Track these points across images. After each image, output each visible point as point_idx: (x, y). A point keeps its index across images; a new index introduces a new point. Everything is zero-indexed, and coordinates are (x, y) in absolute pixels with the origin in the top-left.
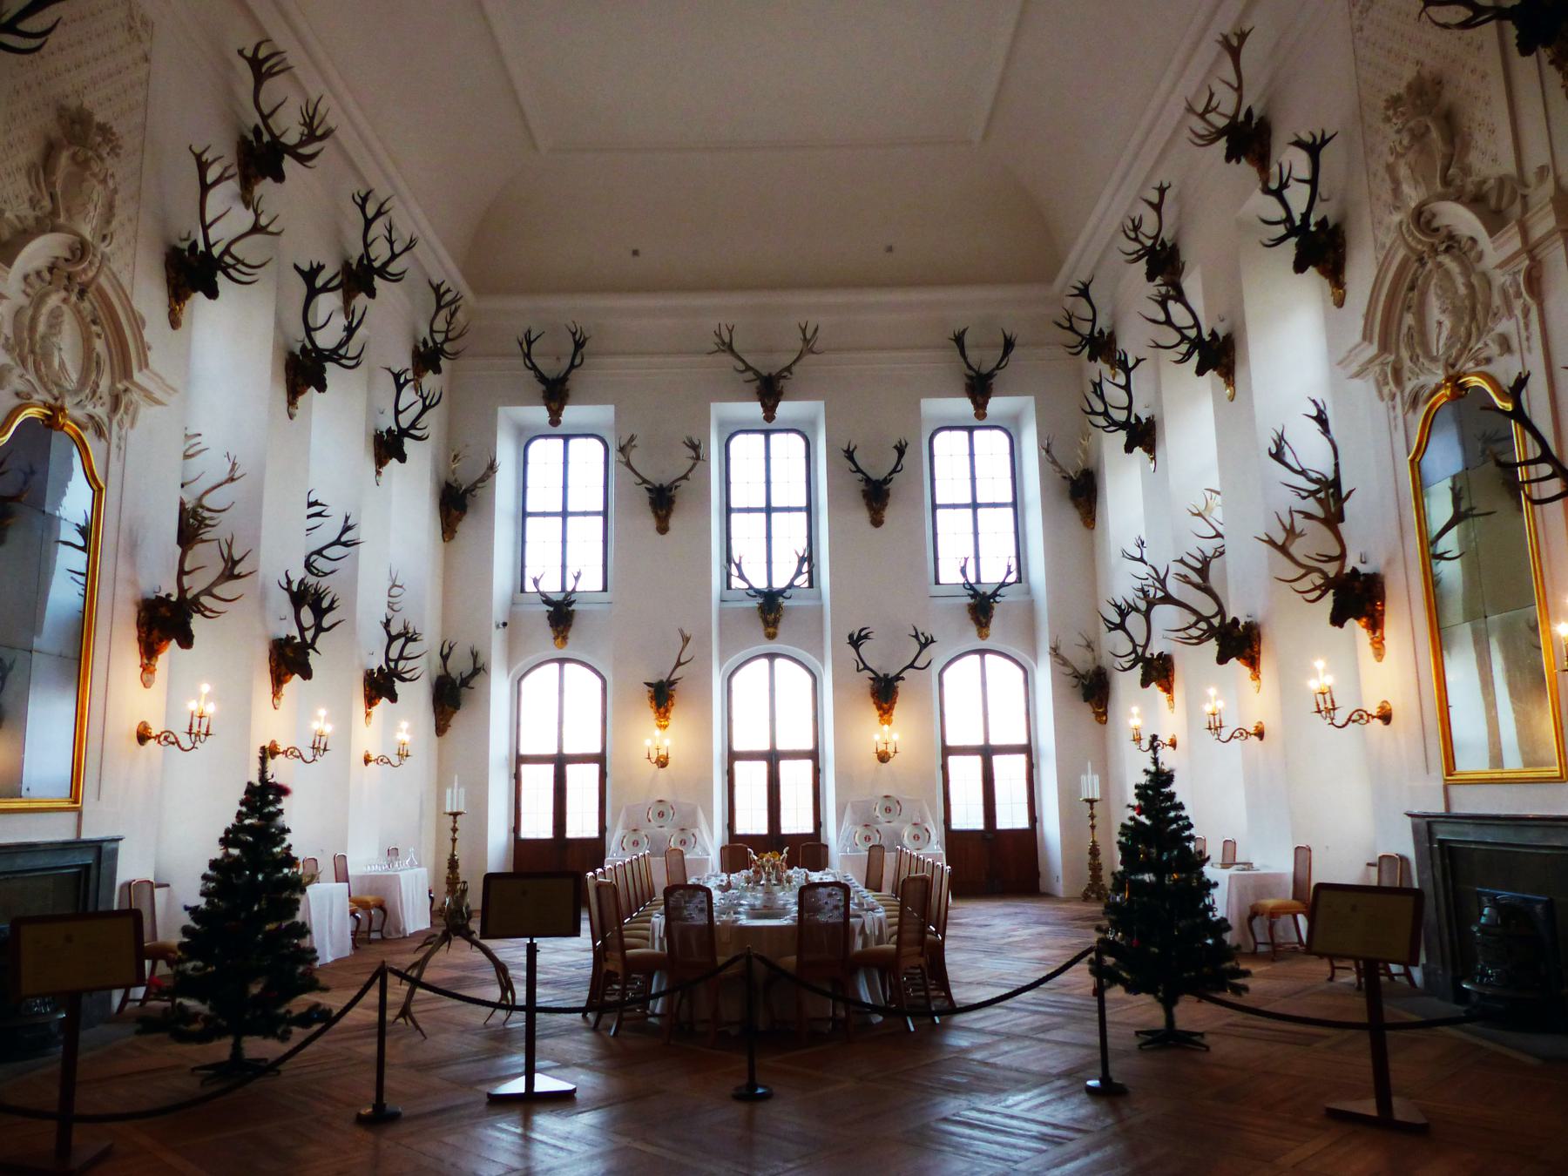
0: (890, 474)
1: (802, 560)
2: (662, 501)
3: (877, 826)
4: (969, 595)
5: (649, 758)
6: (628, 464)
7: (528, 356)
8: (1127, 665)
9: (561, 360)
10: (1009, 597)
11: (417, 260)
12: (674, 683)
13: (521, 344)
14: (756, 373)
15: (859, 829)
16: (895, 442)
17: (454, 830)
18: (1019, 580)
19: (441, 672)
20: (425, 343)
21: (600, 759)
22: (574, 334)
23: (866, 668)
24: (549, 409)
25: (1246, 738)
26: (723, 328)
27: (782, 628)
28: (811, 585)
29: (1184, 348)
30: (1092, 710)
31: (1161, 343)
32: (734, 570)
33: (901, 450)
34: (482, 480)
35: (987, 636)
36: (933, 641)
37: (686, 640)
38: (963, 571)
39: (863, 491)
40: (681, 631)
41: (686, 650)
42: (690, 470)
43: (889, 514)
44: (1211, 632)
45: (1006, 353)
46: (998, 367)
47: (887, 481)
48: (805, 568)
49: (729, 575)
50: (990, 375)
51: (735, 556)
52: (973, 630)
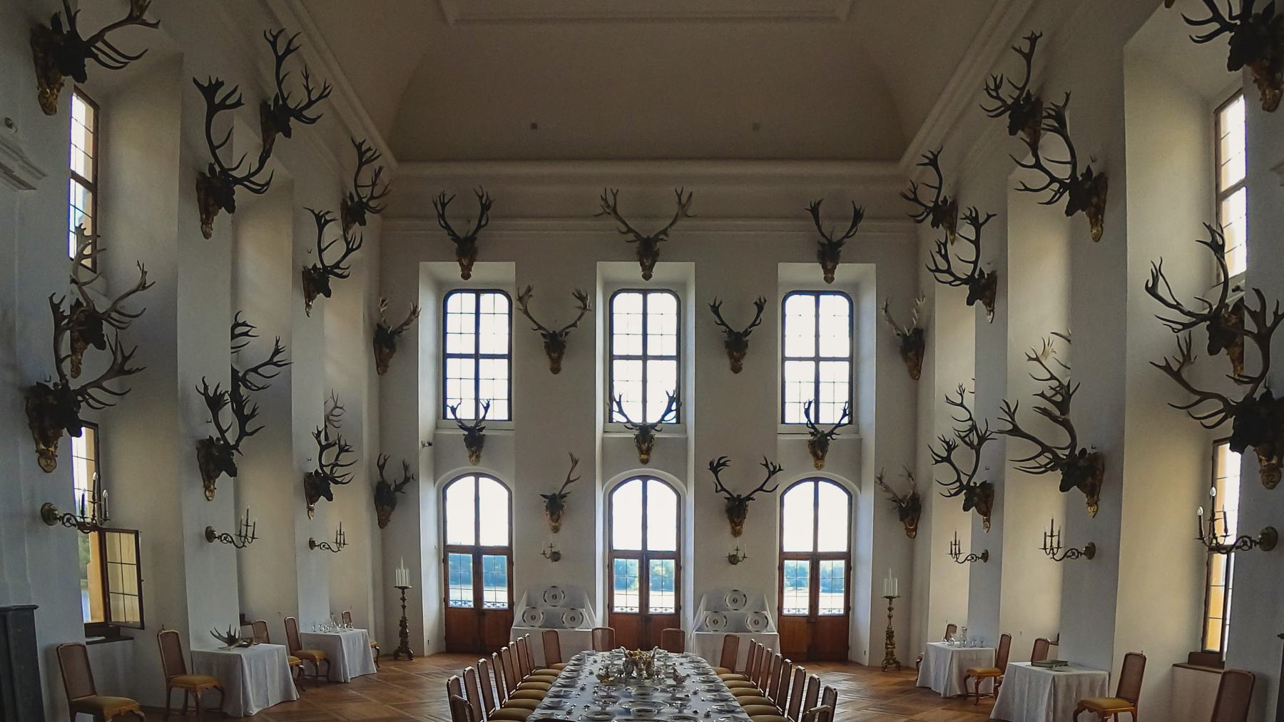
0: (750, 327)
1: (671, 400)
4: (810, 433)
6: (526, 312)
7: (442, 216)
9: (471, 222)
13: (436, 205)
14: (637, 235)
22: (481, 198)
27: (654, 455)
32: (615, 407)
33: (760, 307)
34: (407, 323)
35: (822, 466)
36: (780, 469)
37: (575, 462)
39: (726, 342)
40: (571, 455)
42: (579, 319)
49: (611, 411)
50: (840, 243)
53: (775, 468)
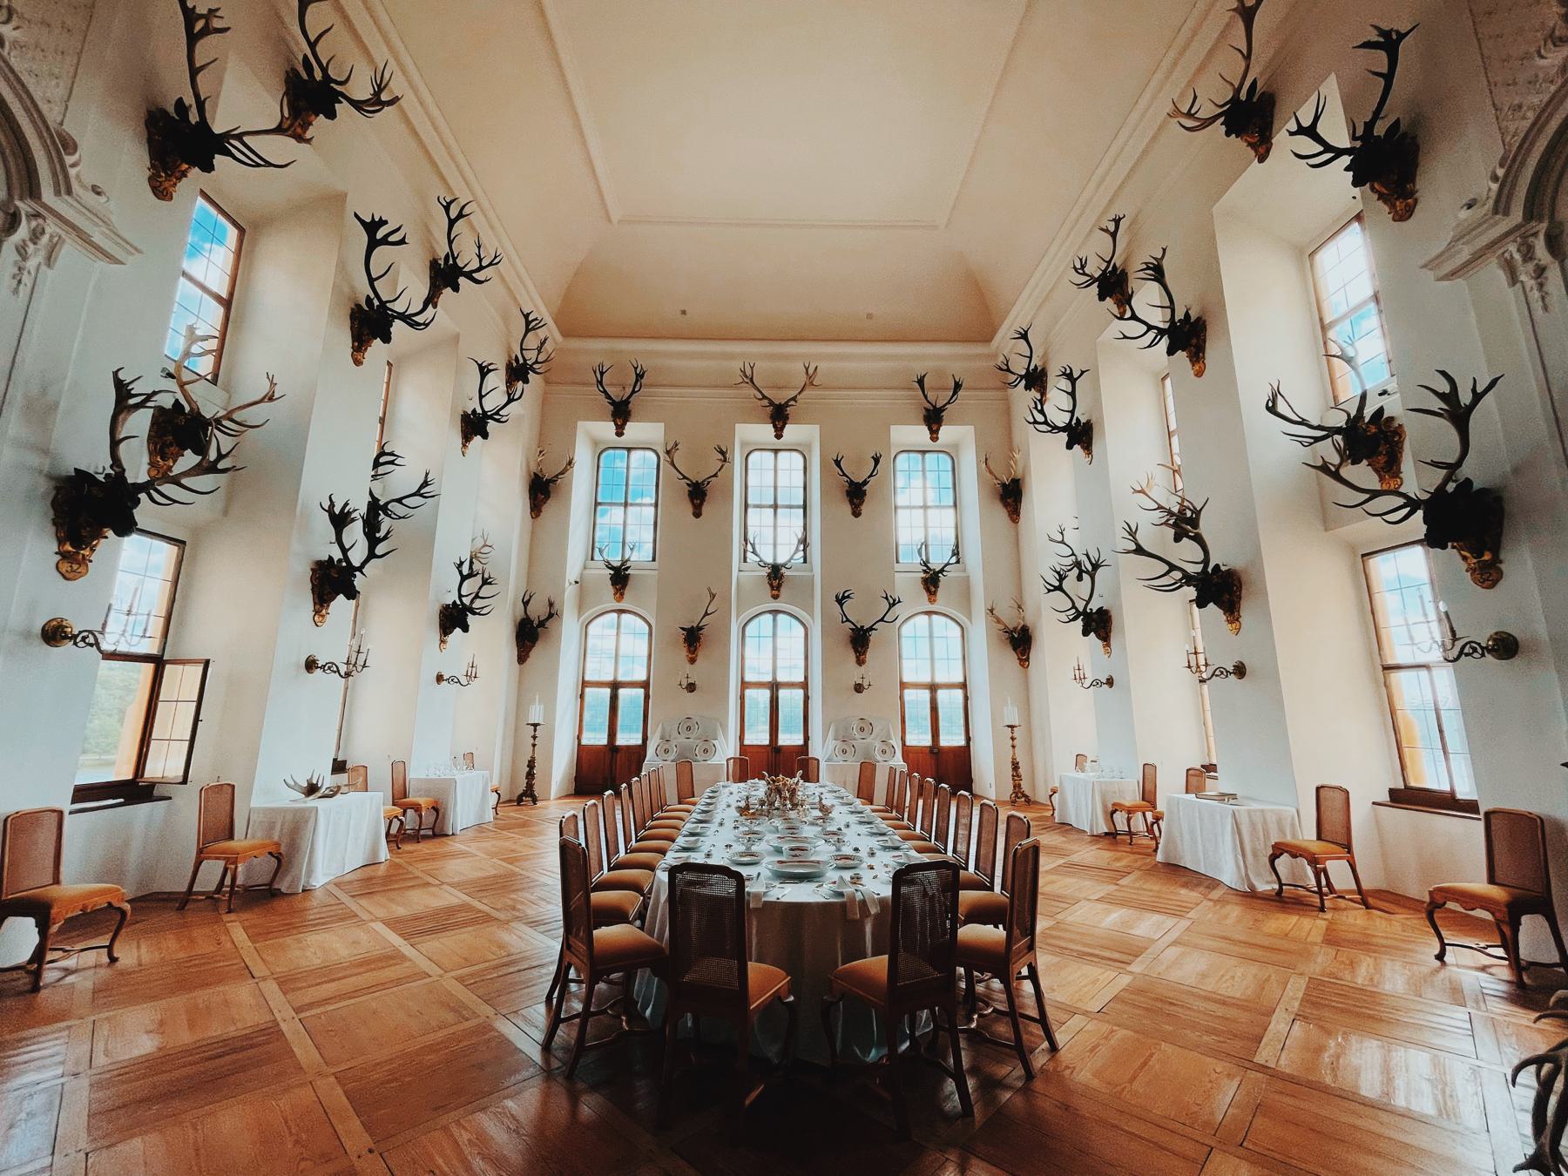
0: (869, 477)
1: (800, 542)
2: (698, 494)
3: (853, 742)
5: (681, 685)
8: (1071, 617)
10: (952, 573)
11: (499, 271)
12: (701, 628)
13: (595, 372)
14: (771, 403)
15: (839, 743)
16: (873, 454)
17: (534, 737)
18: (958, 562)
19: (520, 614)
20: (517, 359)
21: (645, 685)
22: (636, 368)
23: (848, 620)
24: (616, 424)
25: (1227, 676)
26: (747, 365)
28: (805, 561)
29: (1152, 334)
30: (1017, 657)
31: (1128, 335)
32: (749, 548)
33: (877, 460)
35: (935, 601)
36: (899, 602)
37: (713, 596)
38: (920, 555)
39: (847, 491)
40: (709, 590)
41: (712, 604)
42: (719, 470)
43: (864, 508)
44: (1188, 579)
45: (955, 392)
46: (948, 403)
47: (865, 483)
48: (802, 547)
49: (745, 551)
50: (942, 409)
51: (750, 538)
52: (925, 595)
53: (894, 600)
